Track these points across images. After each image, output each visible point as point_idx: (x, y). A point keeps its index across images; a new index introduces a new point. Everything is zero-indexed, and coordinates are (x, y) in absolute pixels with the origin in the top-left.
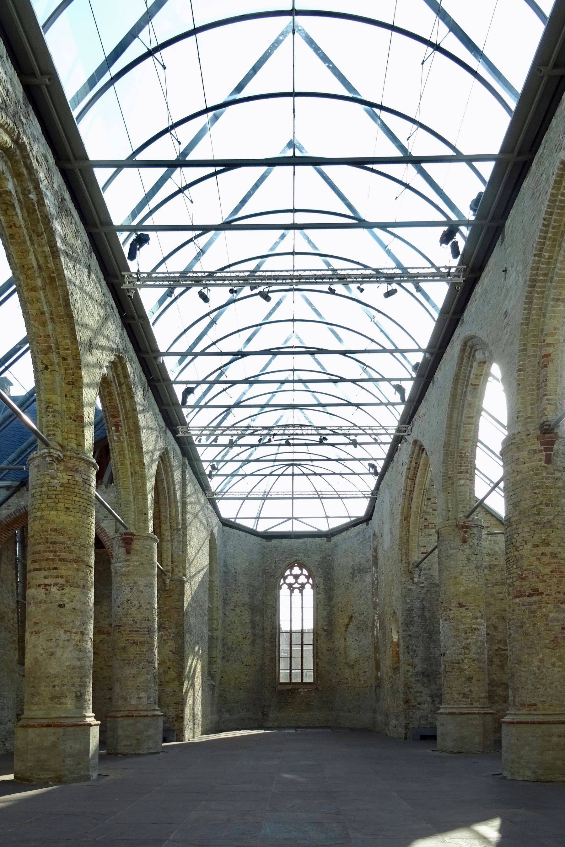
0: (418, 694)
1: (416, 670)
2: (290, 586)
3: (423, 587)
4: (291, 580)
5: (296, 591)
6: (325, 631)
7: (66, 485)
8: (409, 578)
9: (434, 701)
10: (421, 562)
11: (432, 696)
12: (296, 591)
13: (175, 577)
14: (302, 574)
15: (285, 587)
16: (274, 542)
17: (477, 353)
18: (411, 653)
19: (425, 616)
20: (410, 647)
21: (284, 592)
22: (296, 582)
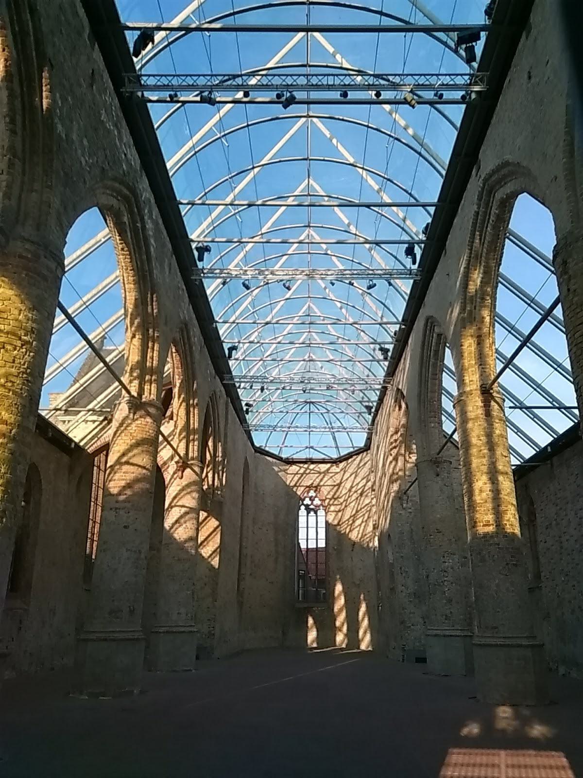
0: (411, 615)
1: (409, 591)
2: (308, 510)
3: (411, 512)
5: (312, 513)
6: (335, 550)
7: (140, 425)
8: (399, 504)
9: (425, 622)
10: (408, 490)
11: (423, 618)
12: (312, 513)
15: (303, 507)
17: (436, 327)
18: (404, 575)
19: (413, 539)
20: (403, 568)
21: (303, 511)
22: (312, 504)
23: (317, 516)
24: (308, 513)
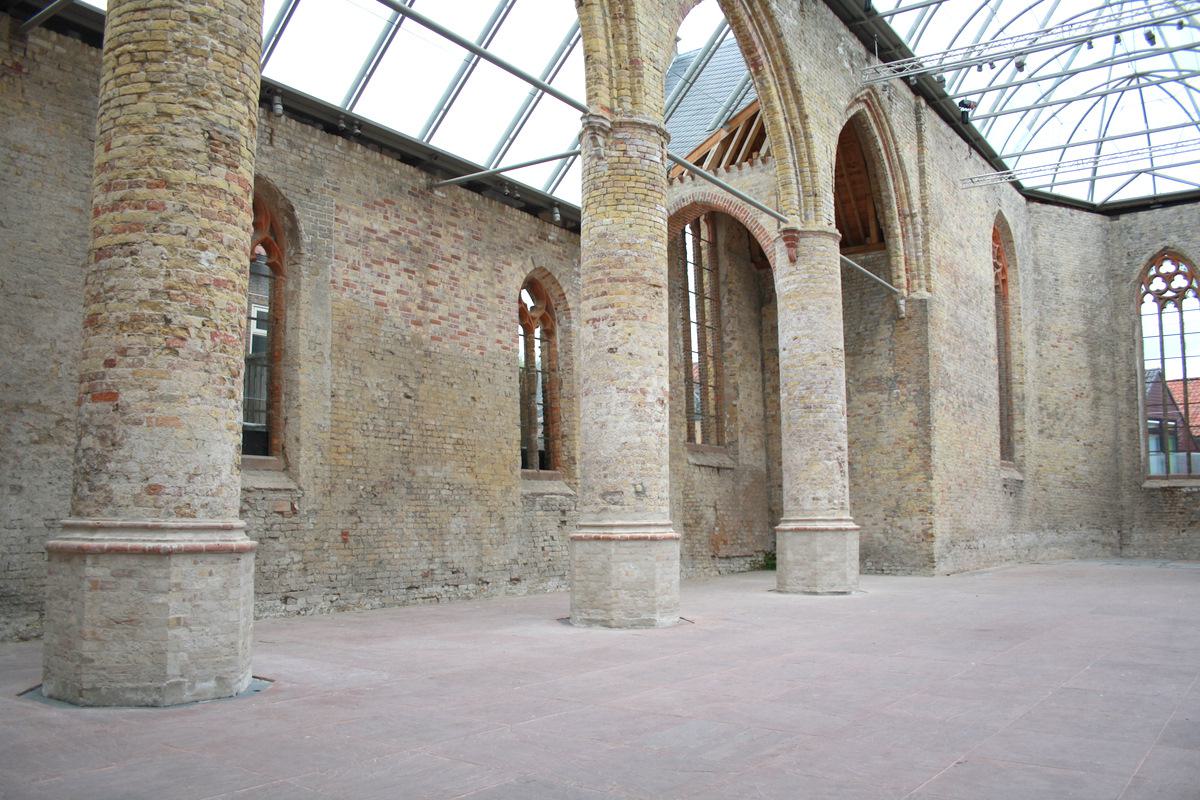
2: (1161, 300)
4: (1158, 284)
5: (1170, 306)
12: (1170, 306)
13: (913, 295)
14: (1177, 272)
15: (1149, 298)
16: (1124, 218)
21: (1149, 306)
23: (1181, 312)
24: (1162, 308)
